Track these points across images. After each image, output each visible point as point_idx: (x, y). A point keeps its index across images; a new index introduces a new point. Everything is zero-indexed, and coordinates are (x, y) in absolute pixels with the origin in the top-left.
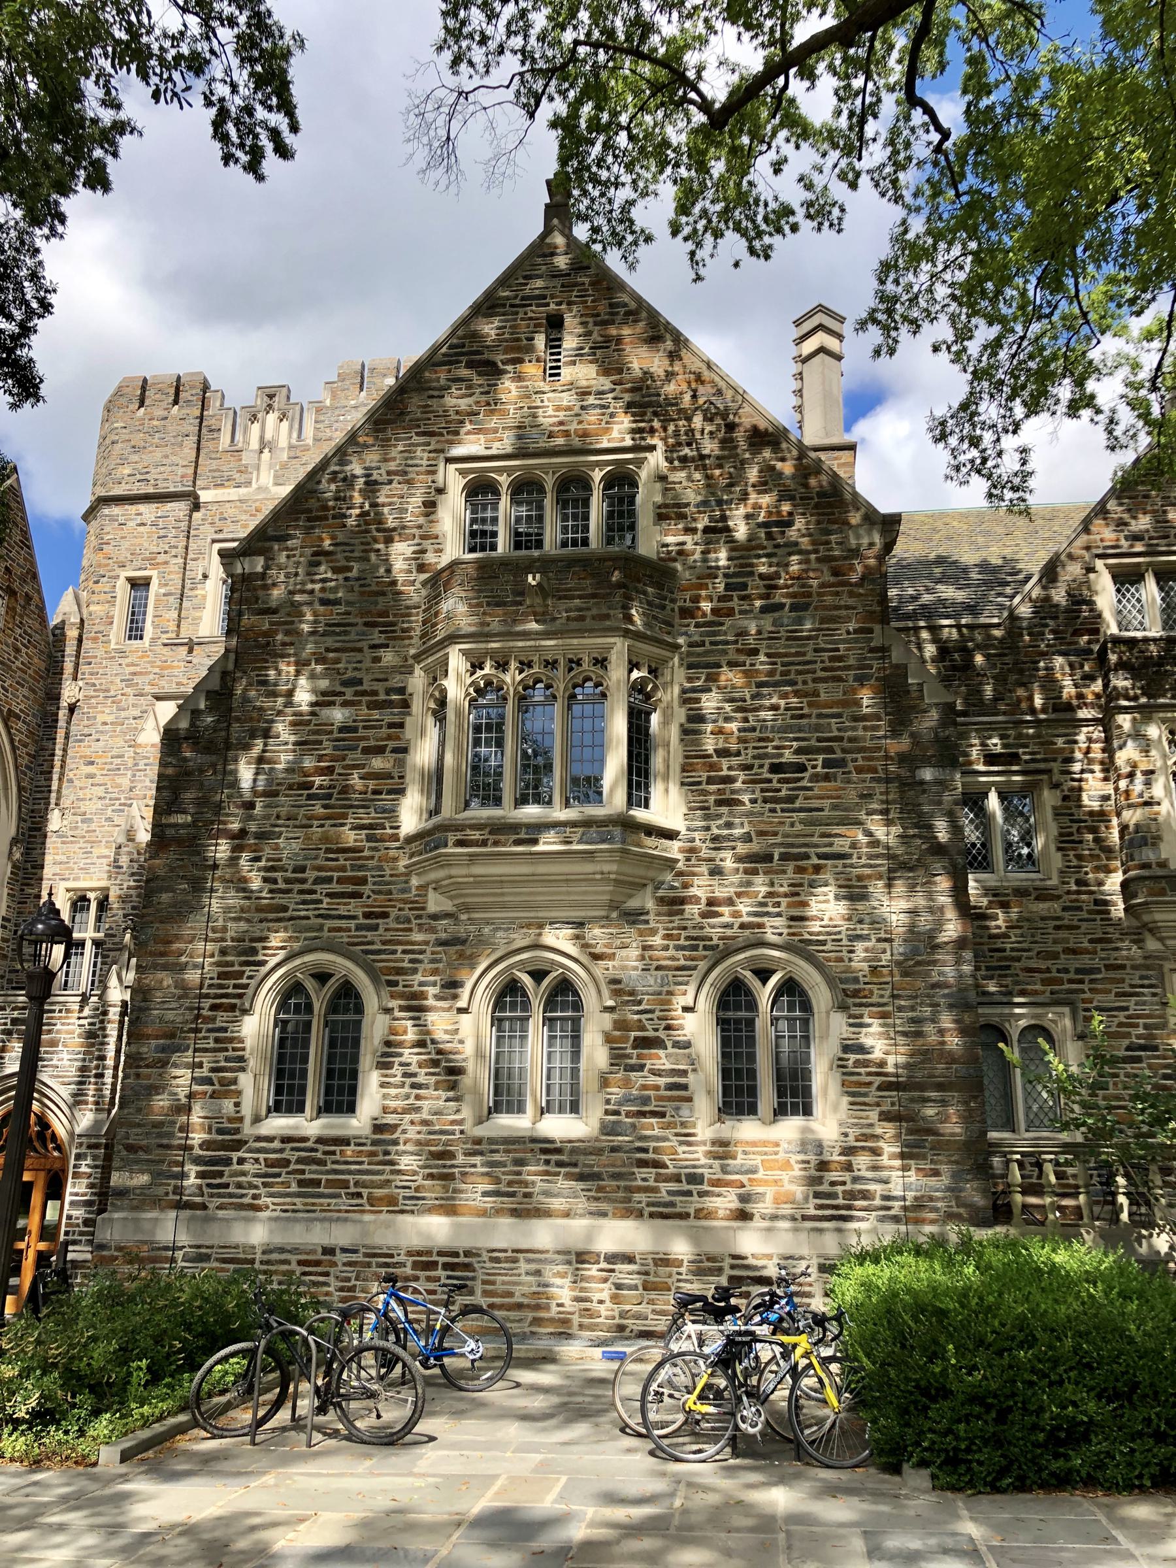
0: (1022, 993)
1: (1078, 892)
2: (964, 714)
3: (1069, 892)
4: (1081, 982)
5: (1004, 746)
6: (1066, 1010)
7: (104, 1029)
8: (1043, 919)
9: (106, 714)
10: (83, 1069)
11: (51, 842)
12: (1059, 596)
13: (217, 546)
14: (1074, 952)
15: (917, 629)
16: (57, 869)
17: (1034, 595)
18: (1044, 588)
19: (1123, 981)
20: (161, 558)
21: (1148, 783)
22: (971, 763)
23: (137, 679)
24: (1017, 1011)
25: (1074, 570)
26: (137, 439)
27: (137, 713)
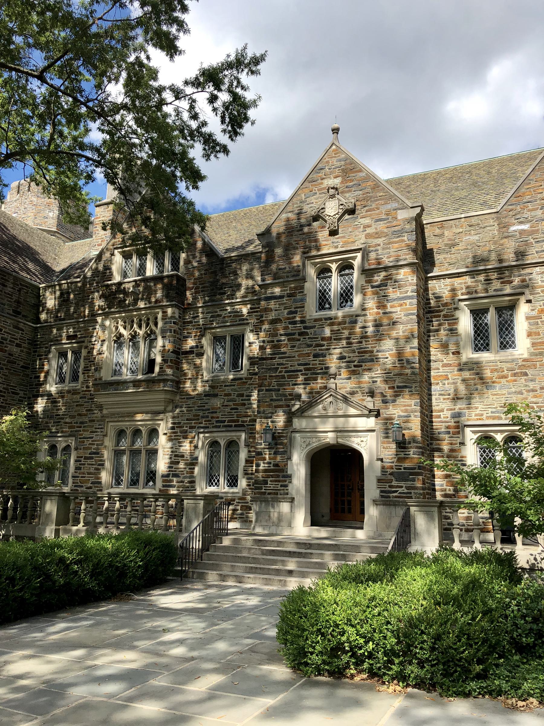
0: (62, 432)
1: (86, 391)
2: (64, 319)
3: (83, 391)
4: (81, 427)
5: (74, 332)
6: (74, 438)
8: (74, 402)
12: (101, 267)
14: (80, 415)
15: (55, 286)
17: (93, 267)
18: (97, 264)
19: (93, 426)
21: (102, 345)
22: (61, 340)
24: (60, 439)
25: (107, 255)
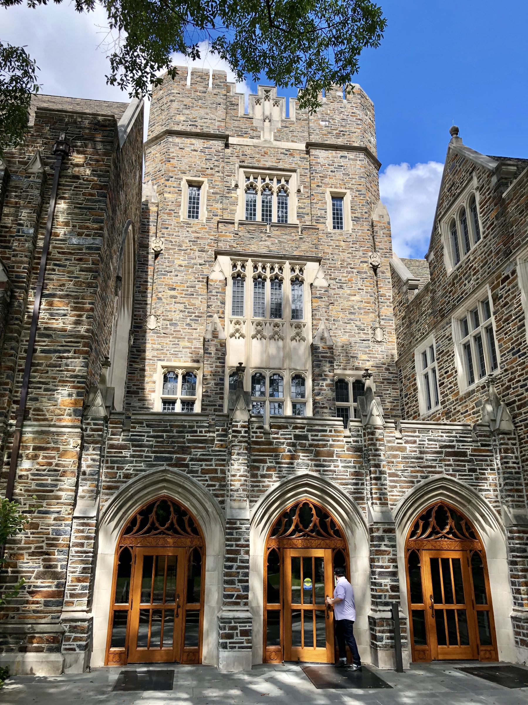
7: (375, 445)
9: (180, 260)
10: (356, 474)
11: (150, 336)
13: (242, 170)
16: (155, 353)
20: (209, 171)
23: (199, 241)
26: (187, 101)
27: (202, 262)
